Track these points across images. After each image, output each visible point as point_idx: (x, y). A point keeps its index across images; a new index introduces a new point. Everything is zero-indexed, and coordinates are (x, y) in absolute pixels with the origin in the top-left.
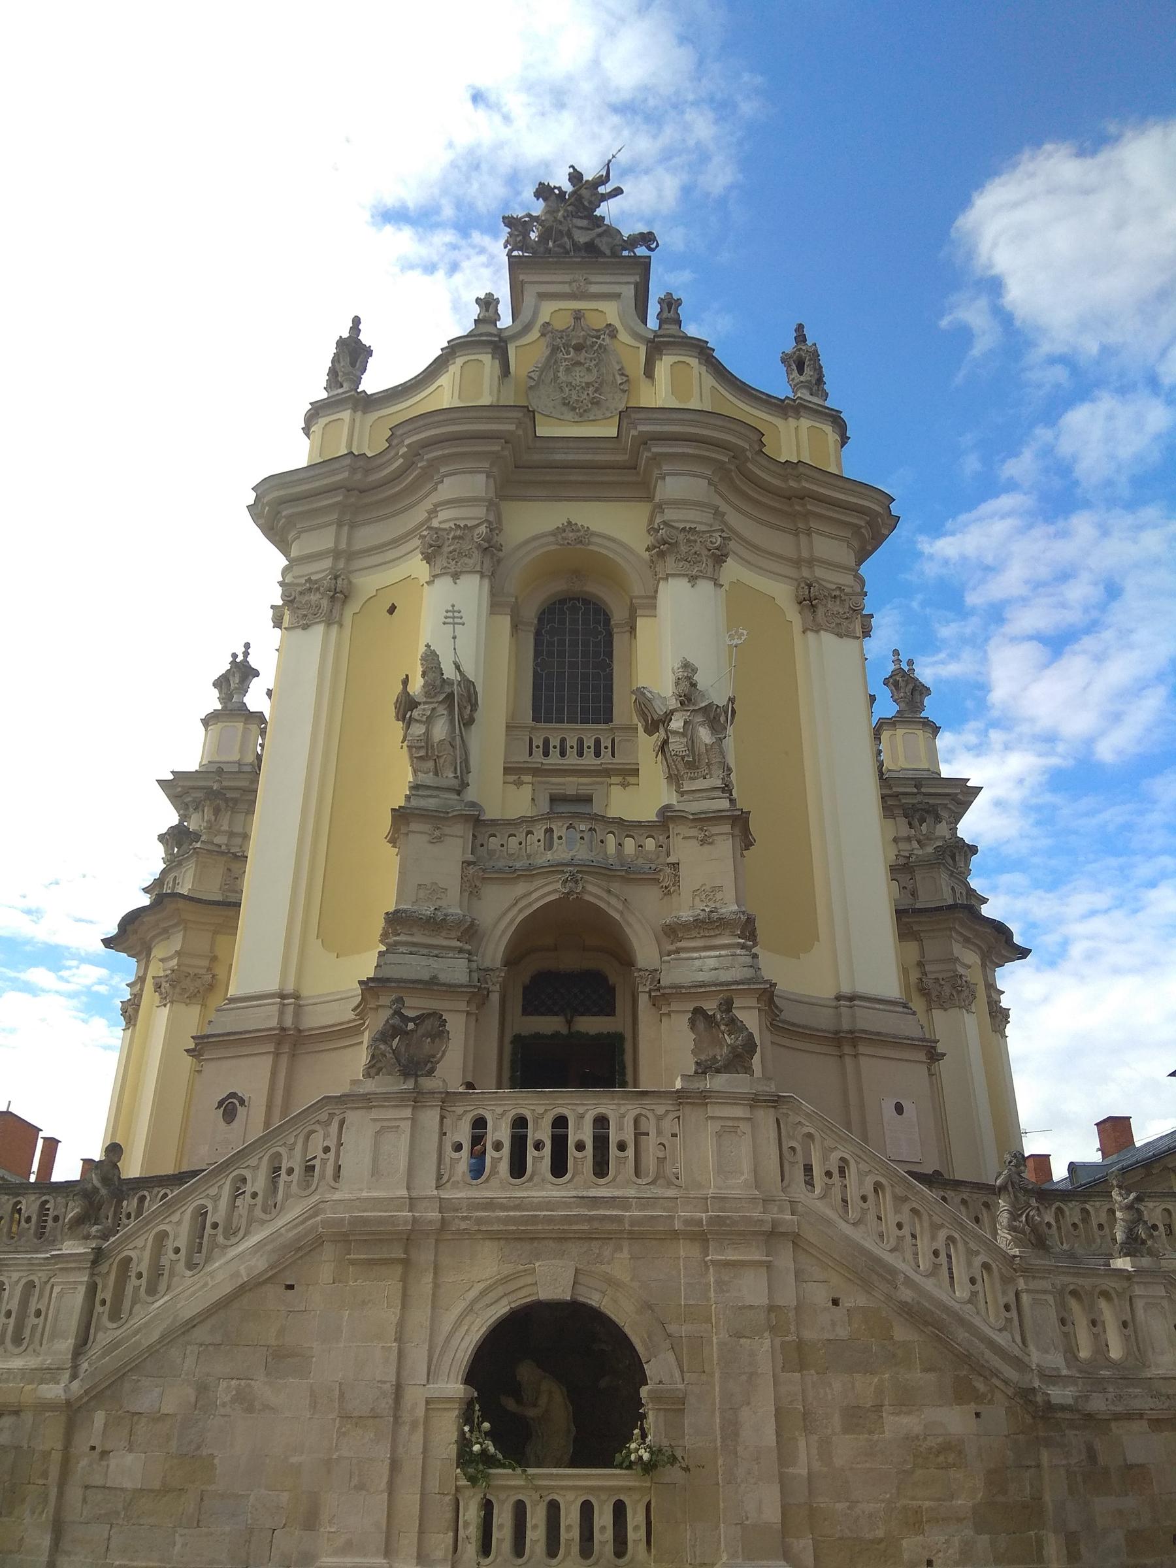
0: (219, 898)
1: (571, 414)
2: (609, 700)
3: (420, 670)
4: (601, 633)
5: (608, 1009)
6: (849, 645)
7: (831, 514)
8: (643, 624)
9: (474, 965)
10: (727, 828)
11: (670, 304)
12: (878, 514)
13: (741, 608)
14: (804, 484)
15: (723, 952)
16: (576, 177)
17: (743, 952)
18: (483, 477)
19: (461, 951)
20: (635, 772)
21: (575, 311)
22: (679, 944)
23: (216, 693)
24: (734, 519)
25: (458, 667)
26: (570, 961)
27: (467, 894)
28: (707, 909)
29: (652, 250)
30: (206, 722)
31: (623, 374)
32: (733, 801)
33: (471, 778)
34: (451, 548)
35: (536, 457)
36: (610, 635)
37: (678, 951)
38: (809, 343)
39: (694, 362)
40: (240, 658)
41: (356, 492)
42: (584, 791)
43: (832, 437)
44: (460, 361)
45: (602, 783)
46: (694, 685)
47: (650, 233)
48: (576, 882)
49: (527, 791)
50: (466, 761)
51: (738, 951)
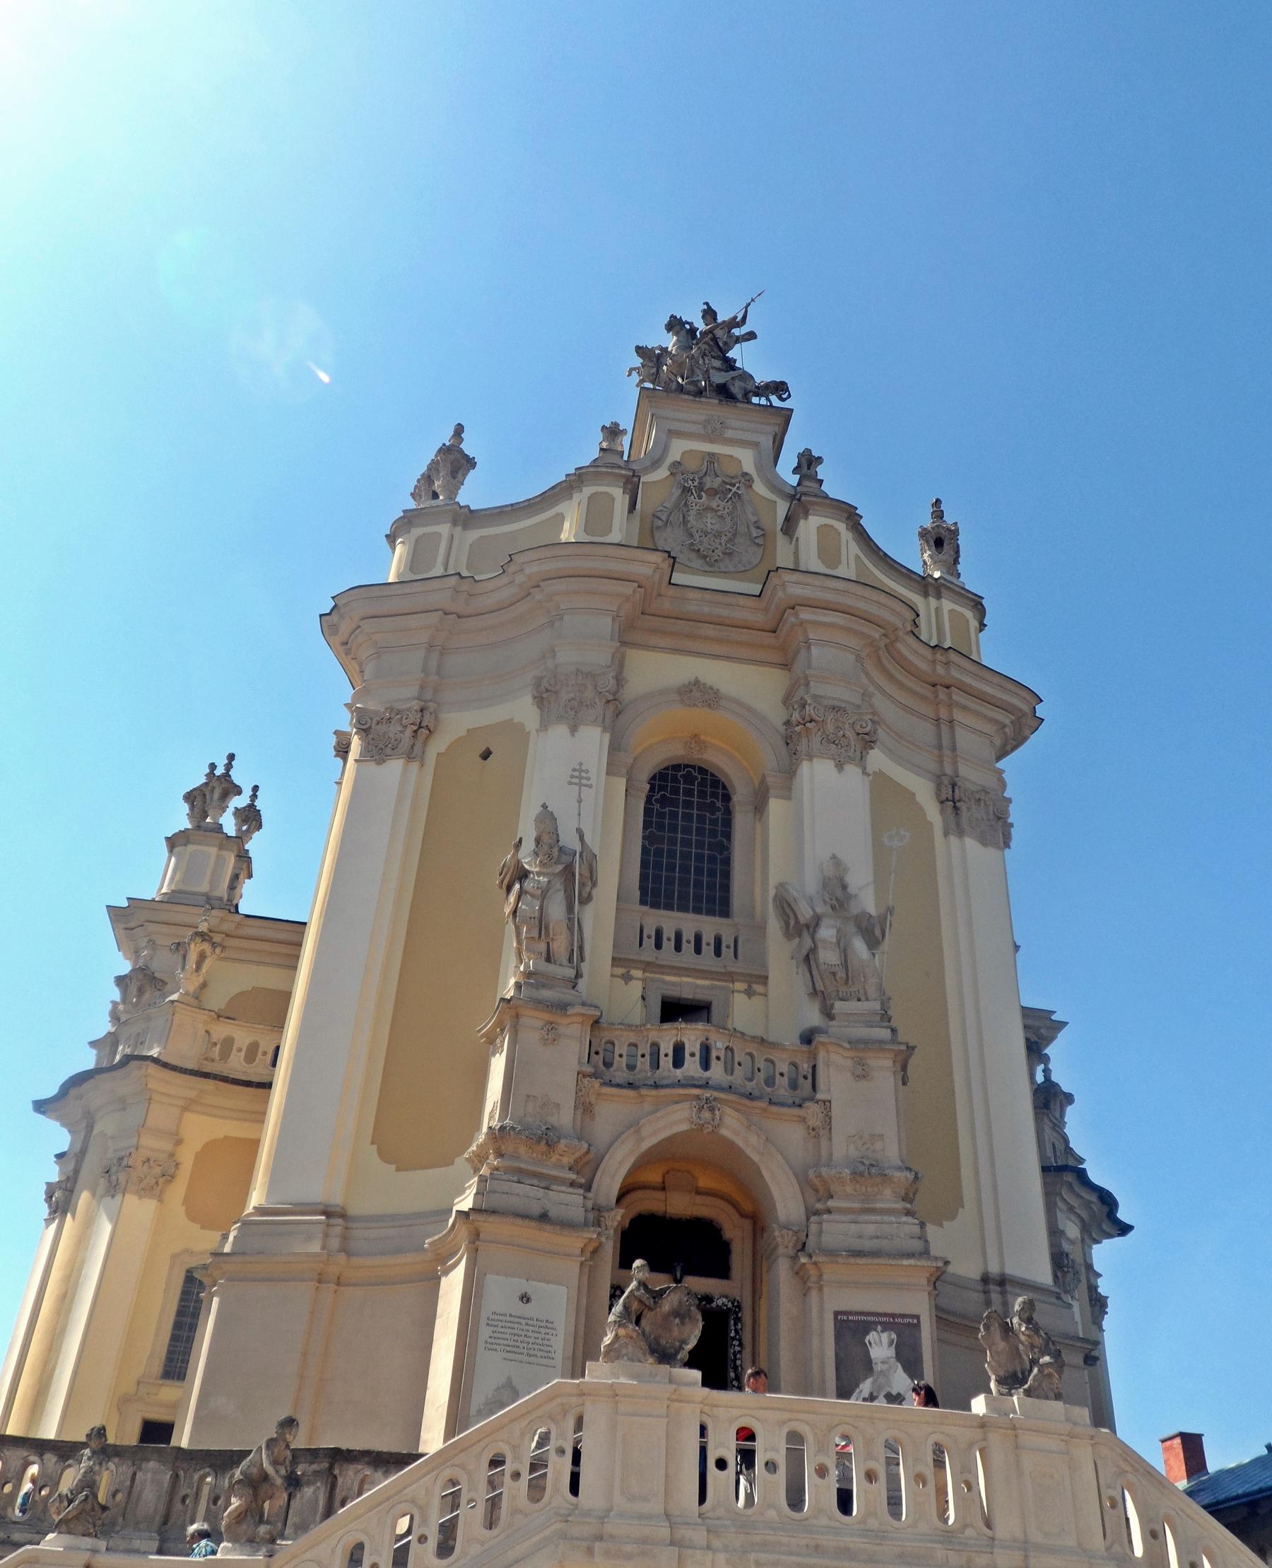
0: (190, 1065)
1: (701, 562)
2: (726, 888)
3: (534, 835)
4: (719, 809)
5: (721, 1270)
6: (991, 853)
7: (978, 708)
8: (775, 806)
9: (590, 1204)
10: (889, 1063)
11: (808, 462)
12: (1024, 715)
13: (886, 799)
14: (954, 673)
15: (886, 1218)
16: (709, 314)
17: (910, 1220)
18: (609, 620)
19: (572, 1184)
20: (764, 980)
21: (709, 454)
22: (830, 1203)
23: (185, 808)
24: (879, 702)
25: (580, 833)
26: (679, 1205)
27: (580, 1112)
28: (867, 1163)
29: (783, 400)
30: (173, 842)
31: (758, 528)
32: (894, 1031)
33: (585, 967)
34: (572, 695)
35: (666, 605)
36: (728, 812)
37: (829, 1211)
38: (949, 519)
39: (841, 527)
40: (220, 771)
41: (454, 616)
42: (701, 996)
43: (974, 624)
44: (588, 490)
45: (722, 988)
46: (844, 887)
47: (783, 383)
48: (712, 1110)
49: (636, 988)
50: (581, 948)
51: (904, 1219)
